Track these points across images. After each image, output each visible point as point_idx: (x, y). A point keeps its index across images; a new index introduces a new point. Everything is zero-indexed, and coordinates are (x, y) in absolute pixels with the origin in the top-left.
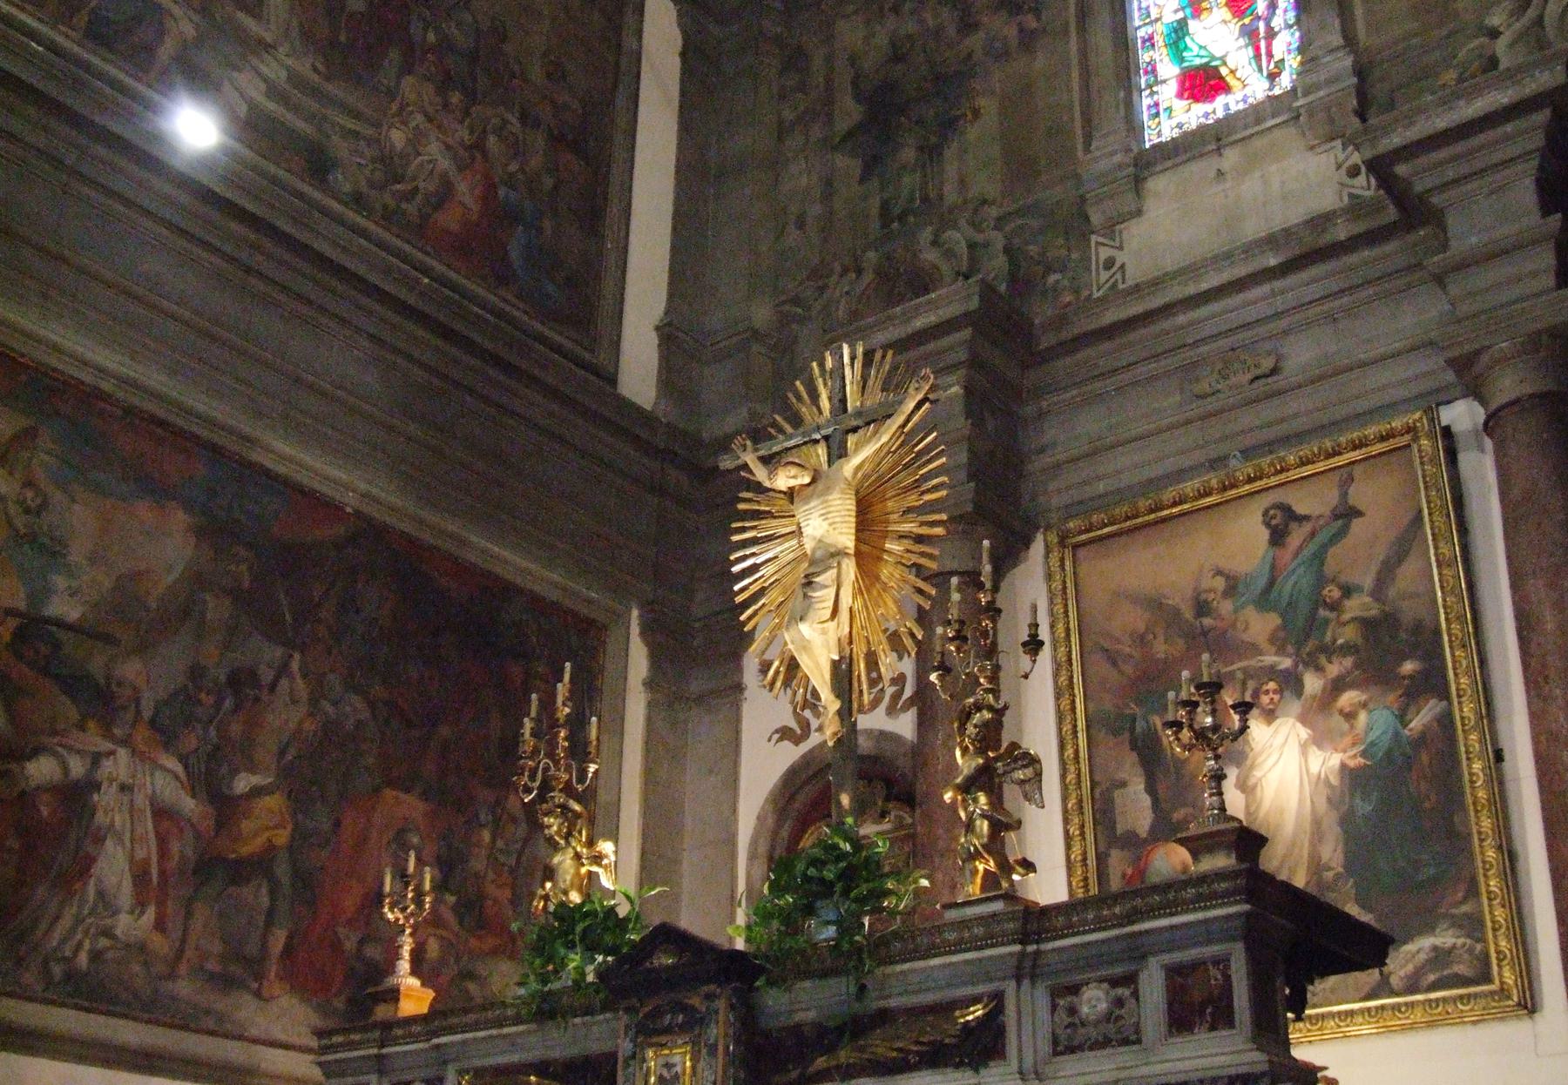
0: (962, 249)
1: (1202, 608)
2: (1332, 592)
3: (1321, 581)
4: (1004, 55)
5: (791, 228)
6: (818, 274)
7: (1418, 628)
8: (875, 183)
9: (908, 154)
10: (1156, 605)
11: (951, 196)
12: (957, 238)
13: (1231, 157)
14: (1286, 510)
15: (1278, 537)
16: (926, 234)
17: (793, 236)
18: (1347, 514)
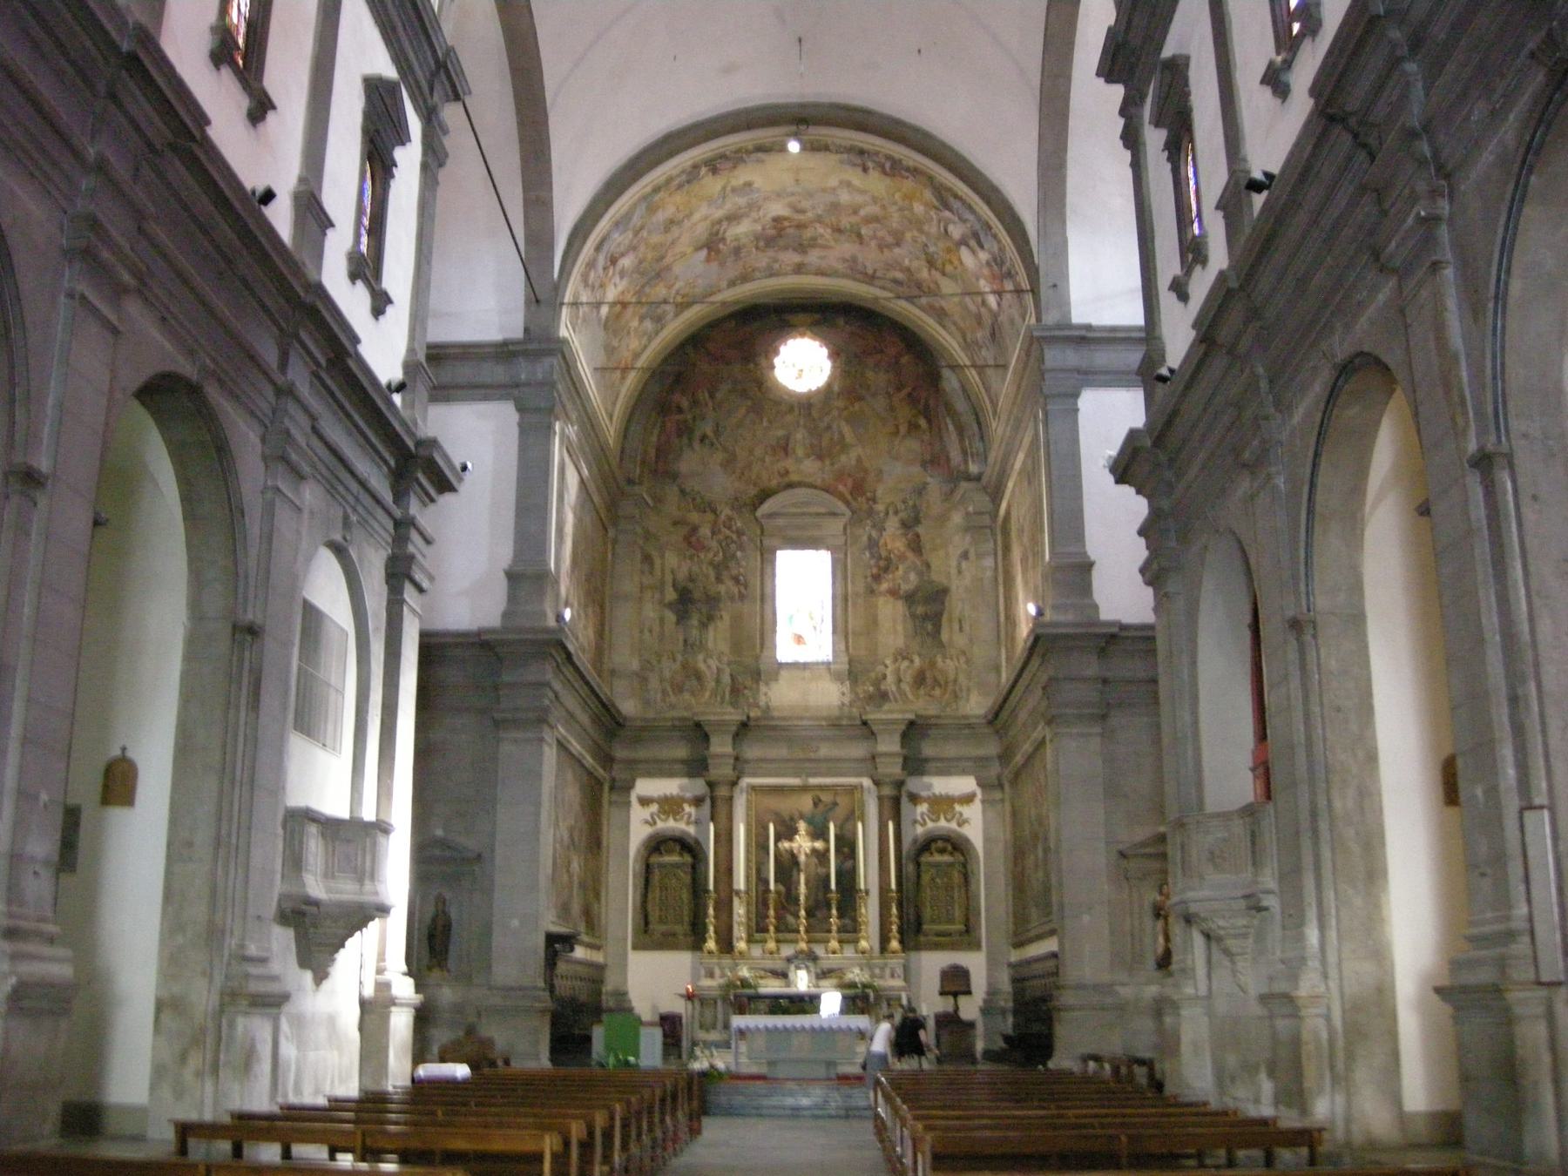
4: (732, 599)
5: (647, 634)
6: (659, 656)
9: (695, 622)
11: (710, 645)
12: (713, 663)
15: (815, 805)
16: (701, 657)
18: (835, 804)
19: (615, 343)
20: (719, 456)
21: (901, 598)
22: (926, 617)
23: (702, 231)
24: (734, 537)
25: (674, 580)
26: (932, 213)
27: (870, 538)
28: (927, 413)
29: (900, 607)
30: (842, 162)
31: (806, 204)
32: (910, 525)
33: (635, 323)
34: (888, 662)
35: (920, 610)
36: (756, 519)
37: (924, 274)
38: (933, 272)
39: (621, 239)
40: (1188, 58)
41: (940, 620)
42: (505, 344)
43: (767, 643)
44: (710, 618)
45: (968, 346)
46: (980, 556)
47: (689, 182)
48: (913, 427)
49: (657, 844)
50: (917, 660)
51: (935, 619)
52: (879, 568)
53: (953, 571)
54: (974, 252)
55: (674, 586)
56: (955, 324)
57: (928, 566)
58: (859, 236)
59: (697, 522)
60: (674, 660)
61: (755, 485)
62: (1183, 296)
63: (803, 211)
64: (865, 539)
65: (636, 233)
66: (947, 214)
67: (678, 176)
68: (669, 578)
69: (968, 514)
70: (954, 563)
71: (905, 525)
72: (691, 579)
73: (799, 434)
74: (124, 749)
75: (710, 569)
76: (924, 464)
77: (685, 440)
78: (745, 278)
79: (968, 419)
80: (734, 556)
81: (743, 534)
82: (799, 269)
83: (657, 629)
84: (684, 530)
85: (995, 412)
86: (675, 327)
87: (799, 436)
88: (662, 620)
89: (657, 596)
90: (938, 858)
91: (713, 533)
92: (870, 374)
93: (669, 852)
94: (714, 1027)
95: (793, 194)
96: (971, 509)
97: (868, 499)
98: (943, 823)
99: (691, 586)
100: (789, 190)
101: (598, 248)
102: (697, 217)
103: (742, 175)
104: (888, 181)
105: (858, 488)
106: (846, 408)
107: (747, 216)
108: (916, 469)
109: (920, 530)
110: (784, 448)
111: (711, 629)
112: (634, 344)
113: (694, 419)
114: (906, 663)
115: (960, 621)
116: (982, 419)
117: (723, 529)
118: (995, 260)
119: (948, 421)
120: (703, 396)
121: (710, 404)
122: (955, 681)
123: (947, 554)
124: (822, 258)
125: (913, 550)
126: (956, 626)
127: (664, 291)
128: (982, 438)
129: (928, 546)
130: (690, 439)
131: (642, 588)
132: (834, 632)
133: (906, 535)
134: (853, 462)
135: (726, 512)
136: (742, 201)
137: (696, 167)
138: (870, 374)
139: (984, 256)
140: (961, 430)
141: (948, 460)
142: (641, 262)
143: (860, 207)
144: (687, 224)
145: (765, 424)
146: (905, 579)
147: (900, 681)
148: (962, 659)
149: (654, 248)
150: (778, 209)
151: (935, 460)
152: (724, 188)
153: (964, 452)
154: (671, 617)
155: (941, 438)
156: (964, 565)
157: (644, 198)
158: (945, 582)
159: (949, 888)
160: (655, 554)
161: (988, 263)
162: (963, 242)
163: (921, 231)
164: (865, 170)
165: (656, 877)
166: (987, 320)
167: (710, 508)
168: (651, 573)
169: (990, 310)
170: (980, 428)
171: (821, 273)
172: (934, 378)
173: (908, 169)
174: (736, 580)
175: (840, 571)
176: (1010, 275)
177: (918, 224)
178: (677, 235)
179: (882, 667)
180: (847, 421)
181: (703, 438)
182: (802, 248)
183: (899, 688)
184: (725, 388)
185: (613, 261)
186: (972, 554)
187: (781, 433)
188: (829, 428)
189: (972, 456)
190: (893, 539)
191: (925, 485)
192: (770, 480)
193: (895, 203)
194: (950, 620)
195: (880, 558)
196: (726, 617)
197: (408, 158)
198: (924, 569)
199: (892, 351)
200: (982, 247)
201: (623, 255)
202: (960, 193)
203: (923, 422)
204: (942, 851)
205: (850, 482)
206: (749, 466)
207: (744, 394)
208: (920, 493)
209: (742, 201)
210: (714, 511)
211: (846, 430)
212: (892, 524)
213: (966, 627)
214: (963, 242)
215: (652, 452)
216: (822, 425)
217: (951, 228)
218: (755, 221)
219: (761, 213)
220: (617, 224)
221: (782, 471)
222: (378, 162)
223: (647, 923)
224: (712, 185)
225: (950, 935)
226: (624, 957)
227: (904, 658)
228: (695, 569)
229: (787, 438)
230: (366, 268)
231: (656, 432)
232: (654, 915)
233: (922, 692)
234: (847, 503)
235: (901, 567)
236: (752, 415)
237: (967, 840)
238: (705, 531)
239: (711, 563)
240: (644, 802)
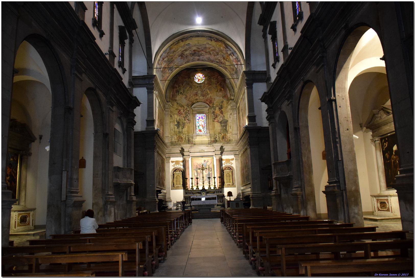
0: (185, 137)
1: (200, 164)
2: (207, 165)
3: (206, 164)
5: (171, 130)
7: (211, 168)
8: (178, 129)
9: (181, 128)
10: (197, 164)
11: (184, 133)
13: (202, 137)
14: (205, 160)
15: (204, 161)
16: (182, 135)
17: (172, 131)
19: (164, 75)
20: (184, 96)
21: (219, 122)
22: (224, 126)
23: (180, 53)
24: (188, 112)
25: (176, 120)
26: (224, 49)
27: (213, 111)
28: (223, 88)
29: (219, 124)
30: (207, 39)
31: (200, 47)
32: (221, 108)
33: (167, 71)
34: (217, 135)
35: (223, 125)
36: (192, 108)
37: (223, 61)
38: (224, 60)
39: (165, 55)
40: (276, 22)
41: (226, 127)
42: (144, 76)
43: (195, 131)
44: (184, 127)
45: (231, 74)
46: (234, 114)
47: (177, 43)
48: (221, 90)
49: (175, 170)
50: (222, 133)
51: (226, 126)
52: (215, 117)
53: (229, 117)
54: (232, 56)
55: (176, 121)
56: (228, 70)
57: (224, 116)
58: (210, 53)
59: (180, 109)
60: (177, 135)
61: (191, 102)
62: (274, 68)
63: (200, 49)
64: (212, 111)
65: (167, 54)
66: (227, 49)
67: (175, 42)
68: (175, 120)
69: (231, 106)
70: (229, 116)
71: (219, 108)
72: (179, 120)
73: (199, 92)
74: (83, 157)
75: (183, 118)
76: (223, 97)
77: (177, 93)
78: (188, 62)
79: (231, 88)
80: (187, 115)
81: (189, 111)
82: (198, 60)
83: (173, 129)
84: (178, 111)
85: (236, 87)
86: (175, 71)
87: (199, 92)
88: (174, 128)
89: (173, 123)
90: (227, 170)
91: (183, 111)
92: (212, 80)
93: (177, 171)
94: (188, 203)
95: (198, 45)
96: (232, 105)
97: (213, 104)
98: (228, 164)
99: (180, 121)
100: (197, 45)
101: (160, 57)
102: (179, 50)
103: (188, 42)
104: (216, 42)
105: (211, 102)
106: (208, 87)
107: (188, 50)
108: (222, 98)
109: (222, 110)
110: (196, 94)
111: (184, 129)
112: (167, 75)
113: (179, 89)
114: (220, 135)
115: (230, 127)
116: (234, 89)
117: (185, 110)
118: (236, 58)
119: (227, 89)
120: (181, 85)
121: (182, 86)
122: (230, 138)
123: (228, 114)
124: (203, 58)
125: (221, 113)
126: (230, 128)
127: (173, 65)
128: (234, 92)
129: (224, 113)
130: (178, 93)
131: (170, 122)
132: (207, 129)
133: (220, 111)
134: (210, 97)
135: (186, 107)
136: (188, 47)
137: (179, 40)
138: (212, 80)
139: (234, 57)
140: (230, 90)
141: (227, 96)
142: (168, 59)
143: (211, 48)
144: (177, 52)
145: (193, 90)
146: (220, 119)
147: (219, 138)
148: (231, 133)
149: (171, 56)
150: (194, 48)
151: (225, 96)
152: (184, 44)
153: (230, 95)
154: (176, 127)
155: (226, 92)
156: (231, 116)
157: (169, 47)
158: (227, 119)
159: (229, 176)
160: (173, 115)
161: (235, 59)
162: (230, 55)
163: (222, 52)
164: (211, 41)
165: (175, 176)
166: (235, 70)
167: (182, 106)
168: (172, 119)
169: (235, 68)
170: (233, 90)
171: (203, 61)
172: (224, 81)
173: (220, 40)
174: (188, 119)
175: (207, 118)
176: (239, 61)
177: (221, 51)
178: (175, 54)
179: (216, 136)
180: (209, 89)
181: (181, 93)
182: (199, 56)
183: (219, 139)
184: (185, 83)
185: (163, 59)
186: (232, 114)
187: (196, 92)
188: (205, 90)
189: (232, 95)
190: (217, 111)
191: (223, 101)
192: (194, 101)
193: (217, 47)
194: (228, 126)
195: (215, 115)
196: (186, 127)
197: (127, 41)
198: (223, 117)
199: (216, 76)
200: (234, 55)
201: (165, 58)
202: (230, 45)
203: (222, 89)
204: (228, 169)
205: (209, 101)
206: (190, 98)
207: (188, 84)
208: (222, 103)
209: (188, 47)
210: (183, 107)
211: (208, 91)
212: (217, 108)
213: (231, 127)
214: (230, 55)
215: (171, 96)
216: (204, 90)
217: (228, 52)
218: (190, 51)
219: (191, 49)
220: (164, 52)
221: (196, 99)
222: (122, 43)
223: (174, 185)
224: (182, 44)
225: (230, 185)
226: (170, 191)
227: (220, 134)
228: (180, 118)
229: (197, 93)
230: (121, 64)
231: (172, 92)
232: (175, 184)
233: (223, 140)
234: (209, 105)
235: (219, 117)
236: (190, 89)
237: (233, 167)
238: (182, 111)
239: (183, 117)
240: (172, 162)
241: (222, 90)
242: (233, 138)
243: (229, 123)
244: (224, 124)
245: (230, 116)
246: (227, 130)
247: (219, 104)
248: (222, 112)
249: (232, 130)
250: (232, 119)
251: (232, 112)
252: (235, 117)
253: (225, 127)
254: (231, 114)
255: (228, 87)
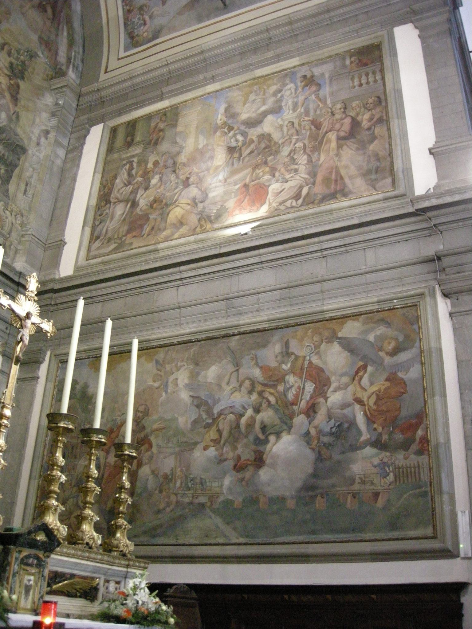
41: (12, 171)
46: (57, 143)
53: (34, 139)
57: (18, 117)
69: (57, 104)
108: (34, 37)
109: (22, 84)
153: (69, 60)
155: (57, 35)
186: (52, 135)
189: (74, 65)
194: (20, 178)
198: (14, 117)
213: (30, 192)
241: (46, 11)
242: (20, 247)
243: (27, 164)
244: (7, 154)
245: (39, 138)
246: (7, 190)
247: (18, 52)
248: (18, 93)
249: (30, 208)
250: (41, 156)
251: (52, 128)
252: (57, 156)
253: (6, 171)
254: (47, 133)
255: (69, 22)
